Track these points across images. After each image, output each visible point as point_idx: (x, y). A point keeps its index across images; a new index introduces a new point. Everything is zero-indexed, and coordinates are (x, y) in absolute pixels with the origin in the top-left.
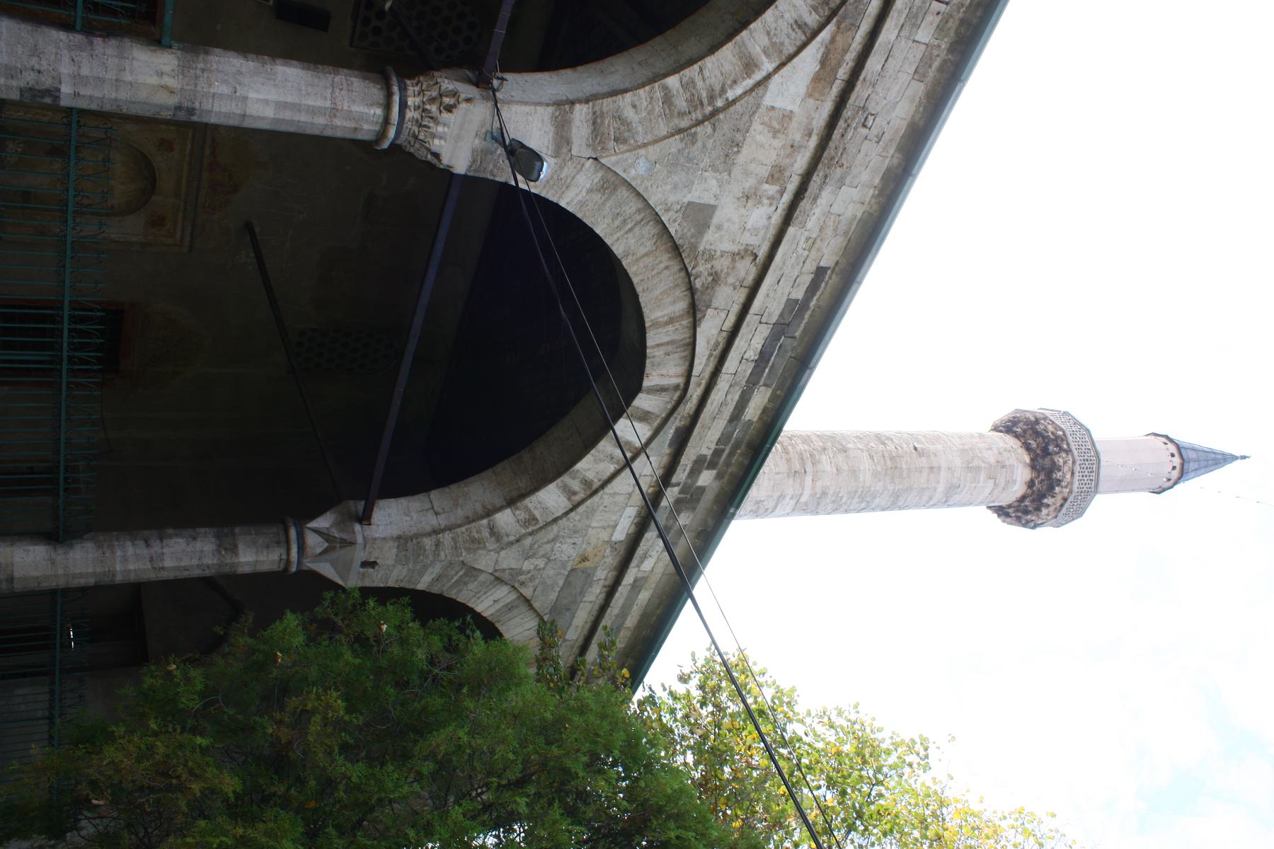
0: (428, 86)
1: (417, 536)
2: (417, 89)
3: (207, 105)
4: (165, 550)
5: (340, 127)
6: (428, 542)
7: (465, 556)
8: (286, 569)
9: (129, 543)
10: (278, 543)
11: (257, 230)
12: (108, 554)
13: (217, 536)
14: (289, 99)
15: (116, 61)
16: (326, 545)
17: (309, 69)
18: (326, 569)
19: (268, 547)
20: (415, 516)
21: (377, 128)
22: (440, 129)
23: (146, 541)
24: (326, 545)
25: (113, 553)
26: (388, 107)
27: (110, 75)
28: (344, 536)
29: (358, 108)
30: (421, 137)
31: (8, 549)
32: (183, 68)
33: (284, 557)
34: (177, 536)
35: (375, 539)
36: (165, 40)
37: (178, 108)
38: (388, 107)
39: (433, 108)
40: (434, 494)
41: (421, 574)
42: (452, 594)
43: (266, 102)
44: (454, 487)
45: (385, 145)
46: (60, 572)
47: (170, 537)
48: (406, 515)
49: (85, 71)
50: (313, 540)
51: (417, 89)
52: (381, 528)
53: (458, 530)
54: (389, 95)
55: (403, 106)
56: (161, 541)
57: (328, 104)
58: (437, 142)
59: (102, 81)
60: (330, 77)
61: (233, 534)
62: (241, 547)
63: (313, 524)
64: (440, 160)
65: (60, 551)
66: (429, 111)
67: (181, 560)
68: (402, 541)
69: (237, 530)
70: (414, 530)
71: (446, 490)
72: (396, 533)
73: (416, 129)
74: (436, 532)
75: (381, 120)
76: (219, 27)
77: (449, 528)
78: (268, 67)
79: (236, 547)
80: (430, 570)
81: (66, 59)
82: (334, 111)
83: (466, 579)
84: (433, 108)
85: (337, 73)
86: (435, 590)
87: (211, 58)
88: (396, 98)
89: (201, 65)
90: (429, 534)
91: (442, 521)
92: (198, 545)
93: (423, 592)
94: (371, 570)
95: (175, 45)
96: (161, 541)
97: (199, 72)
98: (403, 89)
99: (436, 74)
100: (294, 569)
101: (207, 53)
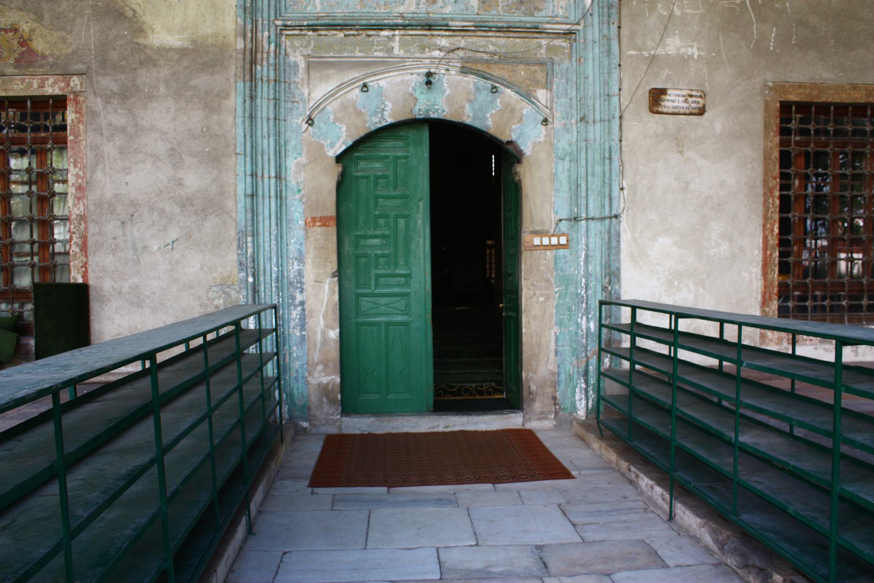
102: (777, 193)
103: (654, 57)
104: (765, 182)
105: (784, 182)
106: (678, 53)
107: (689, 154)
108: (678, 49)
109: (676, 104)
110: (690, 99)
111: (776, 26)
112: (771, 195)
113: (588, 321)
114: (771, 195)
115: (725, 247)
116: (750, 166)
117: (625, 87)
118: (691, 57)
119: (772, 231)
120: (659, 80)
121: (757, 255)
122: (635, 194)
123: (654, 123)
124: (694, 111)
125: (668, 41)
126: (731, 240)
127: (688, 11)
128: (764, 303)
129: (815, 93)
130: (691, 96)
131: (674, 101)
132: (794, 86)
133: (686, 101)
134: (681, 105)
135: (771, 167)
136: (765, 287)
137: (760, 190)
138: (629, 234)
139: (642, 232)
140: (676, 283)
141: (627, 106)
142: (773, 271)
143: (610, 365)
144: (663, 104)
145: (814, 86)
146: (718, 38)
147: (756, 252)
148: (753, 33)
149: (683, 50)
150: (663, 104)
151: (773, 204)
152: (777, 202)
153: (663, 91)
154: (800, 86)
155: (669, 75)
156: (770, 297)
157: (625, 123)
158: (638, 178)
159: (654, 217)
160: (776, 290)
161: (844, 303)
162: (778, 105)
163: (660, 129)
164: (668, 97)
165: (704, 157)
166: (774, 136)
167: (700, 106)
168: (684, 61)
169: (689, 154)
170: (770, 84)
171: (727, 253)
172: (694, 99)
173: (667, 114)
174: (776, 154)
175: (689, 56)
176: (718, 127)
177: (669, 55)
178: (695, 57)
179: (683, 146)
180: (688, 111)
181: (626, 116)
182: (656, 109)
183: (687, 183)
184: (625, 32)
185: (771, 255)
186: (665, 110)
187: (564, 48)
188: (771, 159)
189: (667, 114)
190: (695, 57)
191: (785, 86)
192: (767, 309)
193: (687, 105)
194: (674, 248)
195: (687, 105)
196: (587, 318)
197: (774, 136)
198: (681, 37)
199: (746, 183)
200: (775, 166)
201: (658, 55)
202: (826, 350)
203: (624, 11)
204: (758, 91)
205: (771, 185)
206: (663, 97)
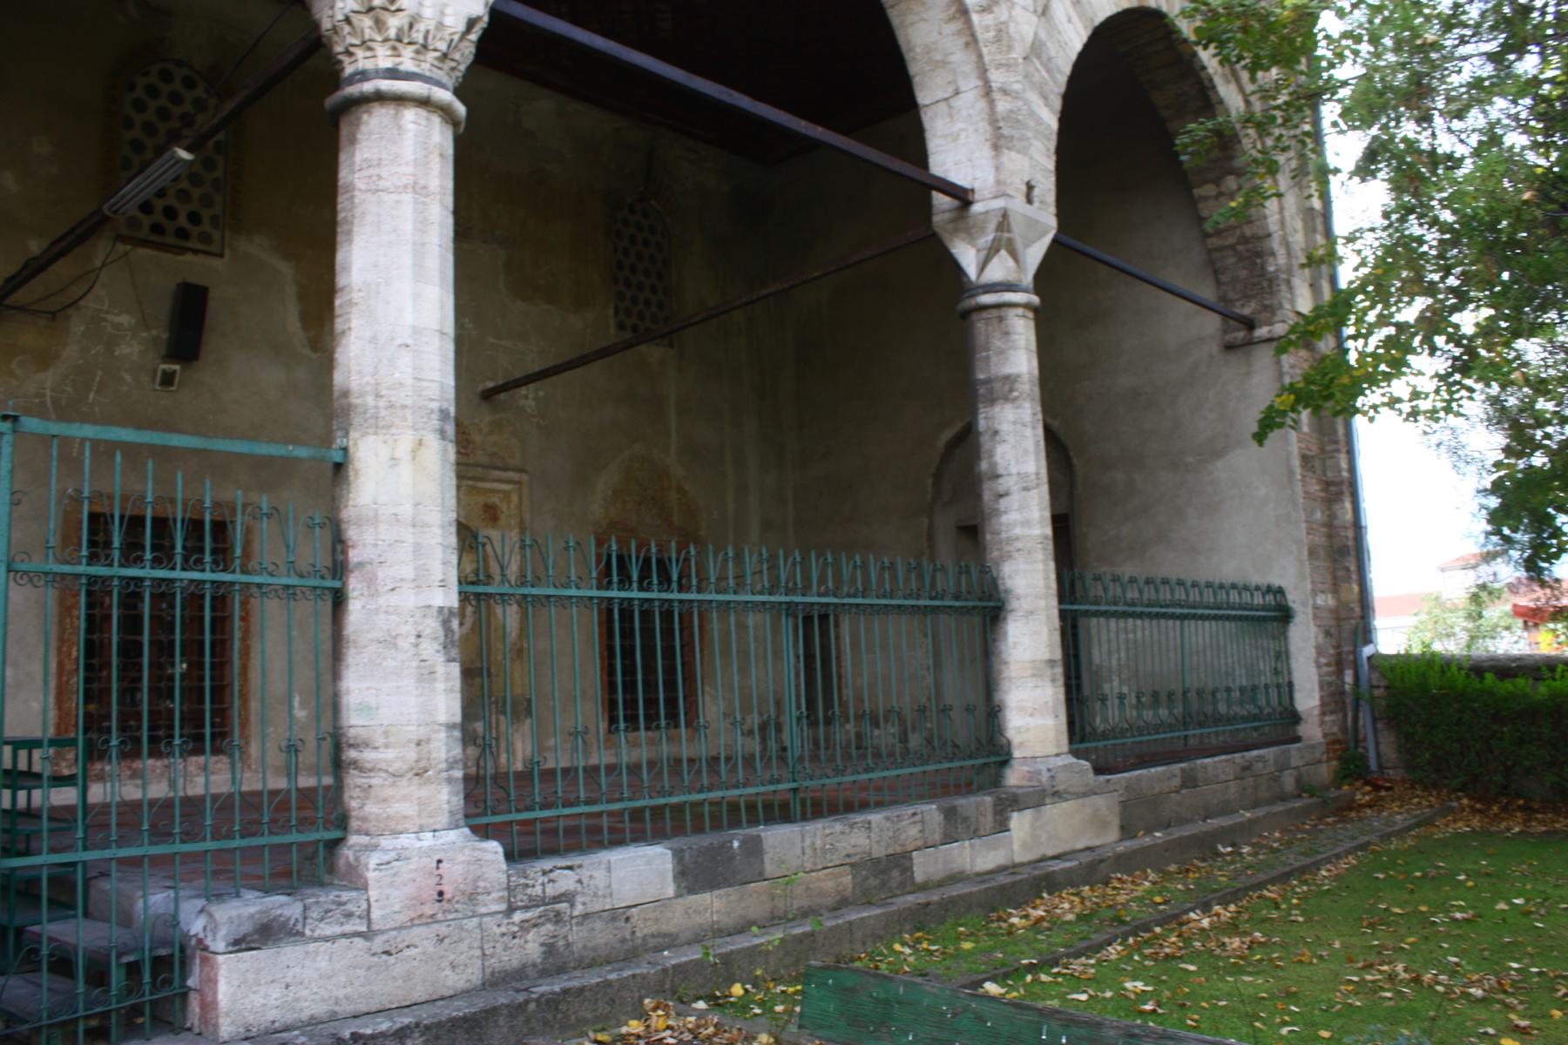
0: (354, 33)
1: (993, 120)
2: (360, 53)
3: (433, 390)
4: (1014, 470)
5: (439, 179)
6: (1002, 105)
7: (1017, 54)
8: (1035, 310)
9: (1004, 519)
10: (1001, 319)
11: (490, 384)
12: (1019, 545)
13: (992, 401)
14: (408, 260)
15: (383, 528)
16: (1003, 253)
17: (349, 233)
18: (1035, 254)
19: (1007, 334)
20: (959, 125)
21: (436, 120)
22: (428, 13)
23: (1001, 496)
24: (1003, 253)
25: (1017, 538)
26: (400, 100)
27: (408, 535)
28: (992, 226)
29: (408, 147)
30: (443, 46)
31: (1013, 667)
32: (378, 425)
33: (1020, 311)
34: (991, 455)
35: (998, 182)
36: (338, 457)
37: (442, 433)
38: (400, 100)
39: (394, 23)
40: (923, 97)
41: (1039, 121)
42: (1063, 79)
43: (416, 297)
44: (913, 69)
45: (461, 109)
46: (1042, 603)
47: (993, 466)
48: (956, 138)
49: (407, 571)
50: (999, 270)
51: (360, 53)
52: (978, 174)
53: (987, 59)
54: (380, 97)
55: (393, 74)
56: (999, 476)
57: (408, 198)
58: (449, 21)
59: (418, 549)
60: (359, 197)
61: (988, 381)
62: (1008, 370)
63: (971, 270)
64: (478, 19)
65: (1014, 604)
66: (400, 30)
67: (1026, 451)
68: (998, 143)
69: (981, 376)
70: (984, 126)
71: (917, 81)
72: (987, 152)
73: (431, 56)
74: (988, 92)
75: (422, 112)
77: (983, 72)
78: (356, 296)
79: (1007, 378)
80: (1035, 108)
81: (393, 599)
82: (418, 189)
83: (1044, 56)
84: (394, 23)
85: (351, 187)
86: (1058, 103)
87: (355, 383)
88: (386, 85)
89: (370, 400)
90: (992, 103)
91: (970, 85)
92: (1005, 427)
93: (1062, 121)
94: (1036, 192)
95: (339, 442)
96: (999, 476)
97: (382, 403)
98: (363, 76)
99: (326, 24)
100: (1035, 299)
101: (346, 394)
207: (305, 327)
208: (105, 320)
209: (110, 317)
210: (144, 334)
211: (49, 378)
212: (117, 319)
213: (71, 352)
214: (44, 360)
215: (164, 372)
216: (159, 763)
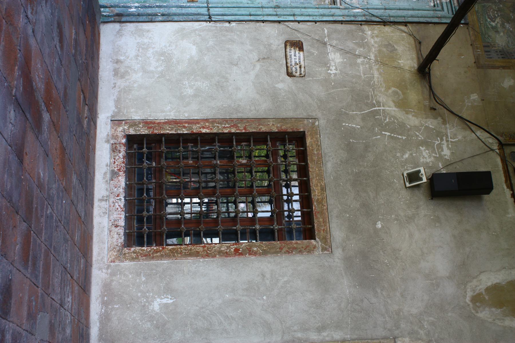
76: (379, 225)
102: (233, 131)
103: (325, 44)
104: (241, 120)
105: (248, 235)
106: (330, 60)
107: (258, 66)
108: (333, 60)
109: (293, 57)
110: (298, 67)
111: (361, 128)
112: (232, 126)
113: (136, 7)
114: (232, 126)
115: (190, 92)
116: (253, 108)
117: (301, 26)
118: (329, 68)
119: (204, 128)
120: (309, 47)
121: (184, 115)
122: (227, 31)
123: (278, 43)
124: (290, 69)
125: (338, 55)
126: (195, 96)
127: (361, 68)
128: (146, 123)
129: (315, 158)
130: (300, 67)
131: (295, 55)
132: (318, 141)
133: (296, 64)
134: (293, 60)
135: (254, 125)
136: (159, 123)
137: (234, 116)
138: (198, 27)
139: (200, 35)
140: (163, 58)
141: (289, 27)
142: (172, 130)
143: (103, 16)
144: (292, 49)
145: (320, 157)
146: (346, 87)
147: (186, 115)
148: (353, 111)
149: (333, 64)
150: (292, 49)
151: (224, 127)
152: (226, 131)
153: (301, 49)
154: (319, 147)
155: (313, 54)
156: (151, 127)
157: (276, 25)
158: (238, 33)
159: (211, 43)
160: (156, 132)
161: (145, 150)
162: (302, 130)
163: (274, 47)
164: (297, 52)
165: (257, 76)
166: (277, 127)
167: (294, 73)
168: (326, 64)
169: (258, 66)
170: (317, 123)
171: (185, 93)
172: (298, 69)
173: (286, 52)
174: (264, 129)
175: (329, 67)
176: (280, 86)
177: (328, 55)
178: (329, 71)
179: (263, 62)
180: (289, 65)
181: (281, 26)
182: (288, 44)
183: (236, 65)
184: (339, 26)
185: (184, 127)
186: (288, 50)
187: (325, 2)
188: (259, 125)
189: (286, 52)
190: (329, 71)
191: (317, 134)
192: (141, 126)
193: (293, 65)
194: (188, 56)
195: (293, 65)
196: (139, 7)
197: (277, 127)
198: (342, 62)
199: (239, 105)
200: (254, 128)
201: (327, 48)
202: (105, 174)
203: (353, 27)
204: (310, 114)
205: (239, 125)
206: (297, 49)
207: (488, 289)
208: (442, 140)
209: (444, 142)
210: (441, 166)
211: (391, 109)
212: (445, 147)
213: (413, 120)
214: (402, 104)
215: (419, 171)
216: (121, 190)
